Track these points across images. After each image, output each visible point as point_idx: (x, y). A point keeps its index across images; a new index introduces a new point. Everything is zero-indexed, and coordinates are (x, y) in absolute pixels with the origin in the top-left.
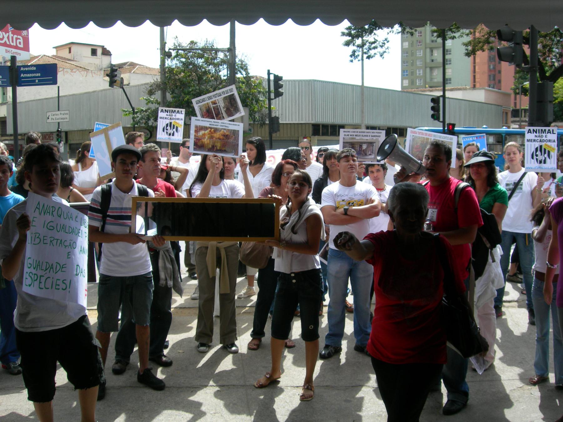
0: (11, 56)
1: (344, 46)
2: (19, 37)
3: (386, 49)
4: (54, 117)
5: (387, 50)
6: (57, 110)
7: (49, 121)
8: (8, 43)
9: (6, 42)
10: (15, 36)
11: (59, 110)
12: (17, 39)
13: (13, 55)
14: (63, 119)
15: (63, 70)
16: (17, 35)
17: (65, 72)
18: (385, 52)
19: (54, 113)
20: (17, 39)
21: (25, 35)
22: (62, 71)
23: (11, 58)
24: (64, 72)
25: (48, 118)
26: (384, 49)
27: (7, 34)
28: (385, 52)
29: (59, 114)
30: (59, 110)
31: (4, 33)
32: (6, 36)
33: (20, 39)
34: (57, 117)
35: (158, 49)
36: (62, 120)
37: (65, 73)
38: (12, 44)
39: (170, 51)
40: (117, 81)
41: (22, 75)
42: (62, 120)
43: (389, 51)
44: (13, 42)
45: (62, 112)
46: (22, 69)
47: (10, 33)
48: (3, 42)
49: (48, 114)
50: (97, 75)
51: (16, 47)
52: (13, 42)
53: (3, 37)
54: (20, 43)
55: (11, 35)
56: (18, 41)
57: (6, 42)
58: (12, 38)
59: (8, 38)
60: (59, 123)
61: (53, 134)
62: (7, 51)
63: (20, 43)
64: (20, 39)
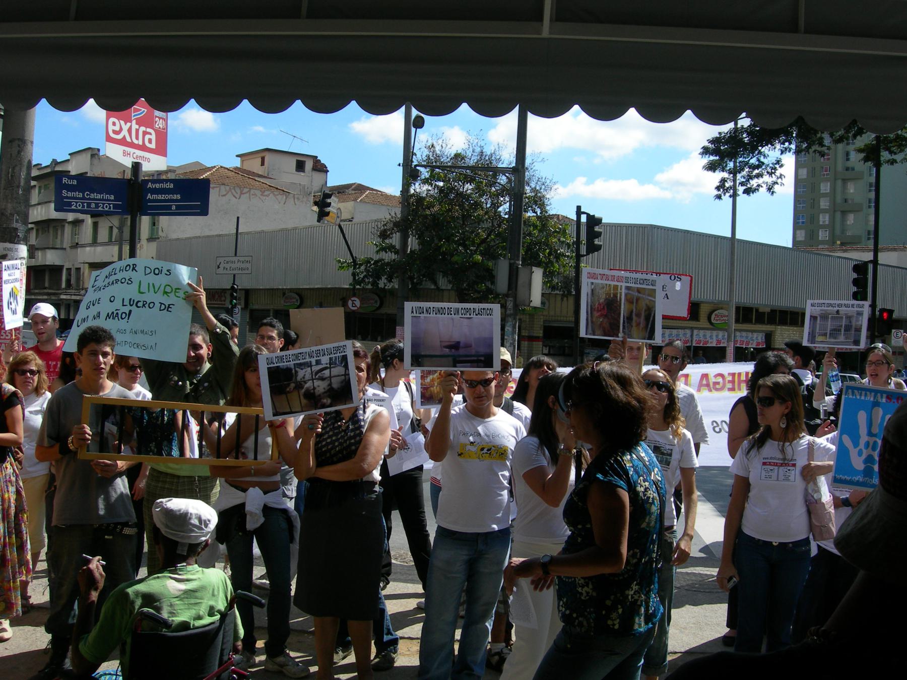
0: (132, 162)
1: (706, 171)
2: (149, 130)
3: (778, 178)
4: (228, 266)
5: (779, 181)
7: (221, 271)
8: (128, 139)
9: (124, 137)
10: (142, 129)
11: (236, 255)
12: (145, 133)
13: (136, 161)
14: (242, 269)
15: (249, 191)
16: (146, 128)
17: (253, 195)
19: (227, 259)
20: (145, 133)
21: (160, 128)
22: (247, 192)
23: (132, 165)
25: (219, 267)
26: (774, 179)
27: (129, 124)
30: (236, 255)
31: (122, 122)
32: (126, 127)
33: (150, 134)
34: (233, 266)
36: (240, 272)
37: (252, 197)
38: (136, 142)
40: (331, 214)
41: (149, 196)
42: (240, 272)
43: (783, 182)
44: (137, 138)
46: (150, 185)
47: (134, 122)
48: (119, 137)
49: (222, 260)
50: (302, 201)
51: (143, 148)
52: (137, 138)
53: (121, 129)
54: (150, 141)
55: (135, 126)
56: (147, 137)
57: (124, 137)
58: (137, 131)
59: (130, 131)
61: (226, 293)
62: (125, 154)
63: (150, 141)
64: (150, 134)
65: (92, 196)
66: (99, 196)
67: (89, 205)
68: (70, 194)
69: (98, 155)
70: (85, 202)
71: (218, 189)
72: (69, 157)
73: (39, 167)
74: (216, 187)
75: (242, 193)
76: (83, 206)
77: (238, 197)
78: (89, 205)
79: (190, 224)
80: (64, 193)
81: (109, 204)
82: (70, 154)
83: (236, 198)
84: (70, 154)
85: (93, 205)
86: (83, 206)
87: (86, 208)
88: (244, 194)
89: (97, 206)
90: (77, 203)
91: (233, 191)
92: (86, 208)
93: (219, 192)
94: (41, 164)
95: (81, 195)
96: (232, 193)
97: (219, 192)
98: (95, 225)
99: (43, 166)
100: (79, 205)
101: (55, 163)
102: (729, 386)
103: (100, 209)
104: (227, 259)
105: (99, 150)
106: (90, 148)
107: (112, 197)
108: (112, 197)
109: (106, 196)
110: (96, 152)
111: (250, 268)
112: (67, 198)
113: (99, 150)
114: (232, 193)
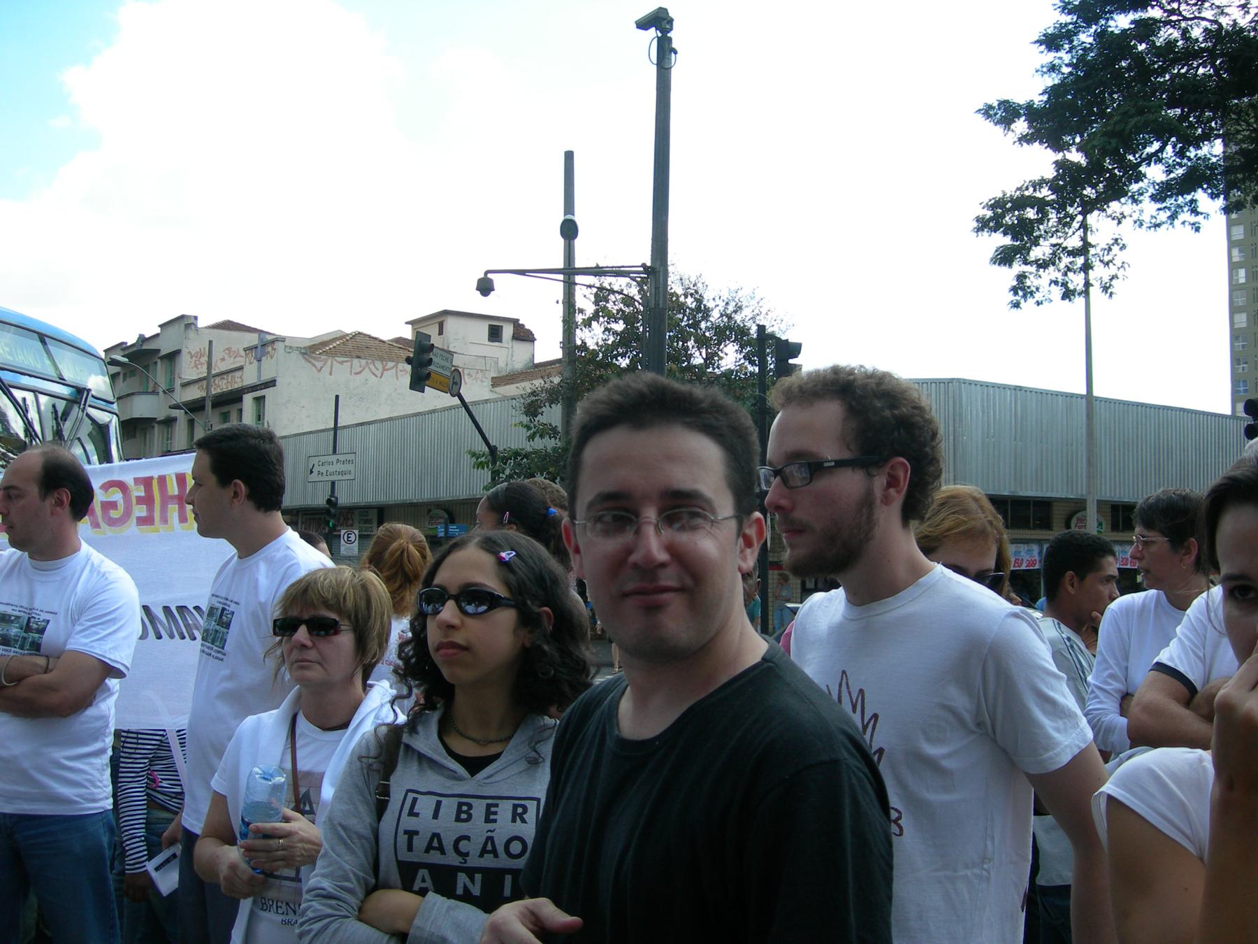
3: (1119, 268)
4: (323, 469)
5: (1120, 273)
6: (331, 452)
7: (314, 477)
11: (334, 452)
14: (342, 473)
15: (396, 366)
17: (401, 371)
18: (1114, 277)
19: (323, 459)
22: (393, 368)
24: (396, 372)
25: (311, 472)
26: (1112, 270)
28: (1114, 277)
29: (335, 463)
30: (334, 452)
34: (331, 469)
35: (557, 302)
36: (340, 477)
37: (400, 374)
39: (490, 276)
40: (432, 375)
42: (340, 477)
43: (1126, 274)
45: (341, 458)
49: (315, 461)
50: (476, 379)
60: (333, 483)
61: (353, 513)
69: (195, 325)
71: (349, 363)
72: (158, 330)
73: (124, 346)
74: (346, 361)
75: (384, 369)
77: (379, 375)
79: (308, 417)
82: (159, 326)
83: (377, 376)
84: (159, 326)
88: (387, 370)
91: (372, 366)
93: (351, 367)
94: (126, 343)
96: (370, 370)
97: (351, 367)
98: (191, 423)
99: (128, 344)
101: (142, 339)
102: (140, 511)
104: (323, 459)
105: (196, 318)
106: (182, 317)
110: (193, 321)
111: (353, 472)
113: (196, 318)
114: (370, 370)
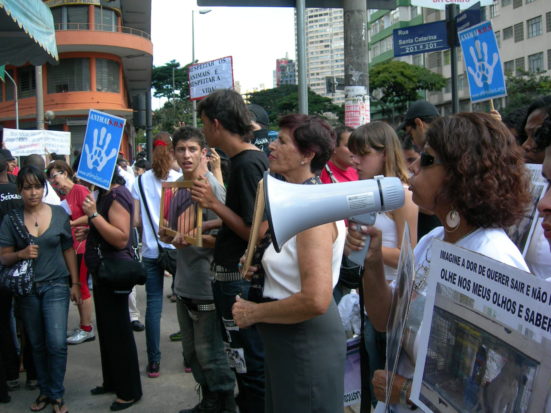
0: (446, 5)
23: (446, 8)
65: (421, 39)
66: (425, 39)
67: (418, 47)
68: (404, 42)
70: (415, 46)
76: (414, 49)
78: (418, 47)
80: (400, 42)
81: (433, 43)
85: (421, 47)
86: (414, 49)
87: (416, 50)
89: (424, 46)
90: (409, 47)
92: (416, 50)
95: (412, 41)
100: (411, 49)
103: (427, 48)
107: (435, 37)
108: (435, 37)
109: (430, 38)
112: (402, 45)
